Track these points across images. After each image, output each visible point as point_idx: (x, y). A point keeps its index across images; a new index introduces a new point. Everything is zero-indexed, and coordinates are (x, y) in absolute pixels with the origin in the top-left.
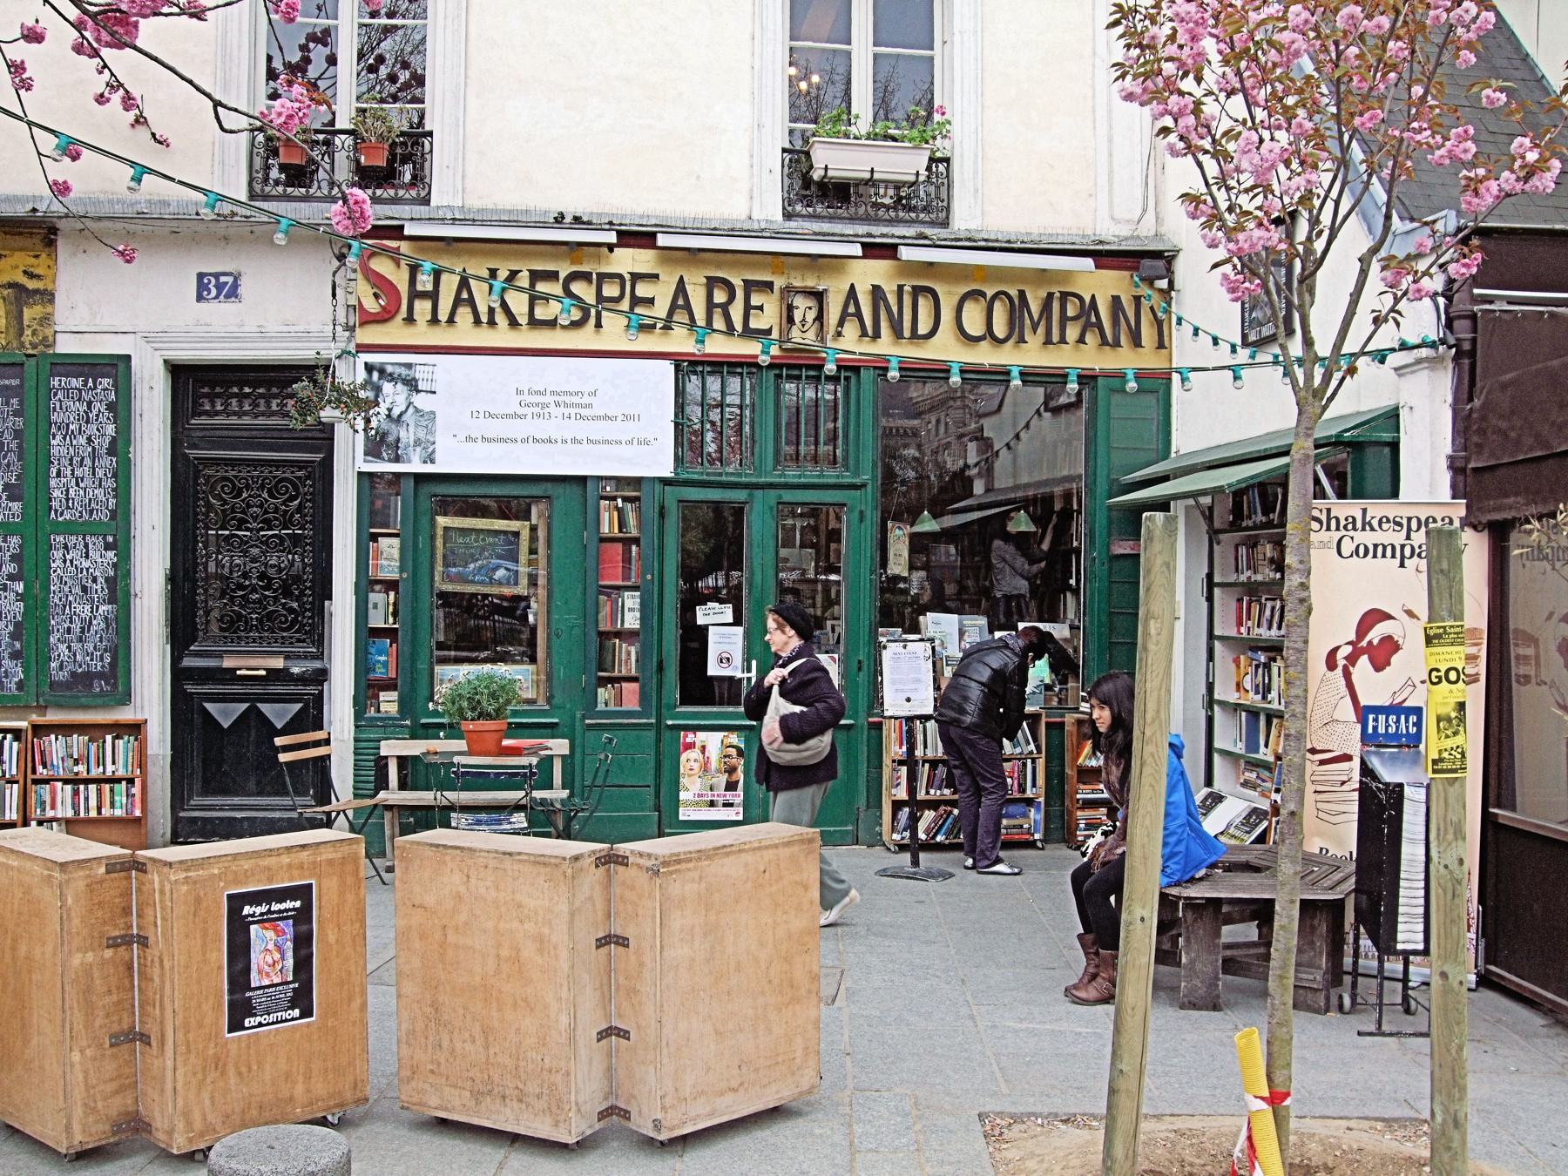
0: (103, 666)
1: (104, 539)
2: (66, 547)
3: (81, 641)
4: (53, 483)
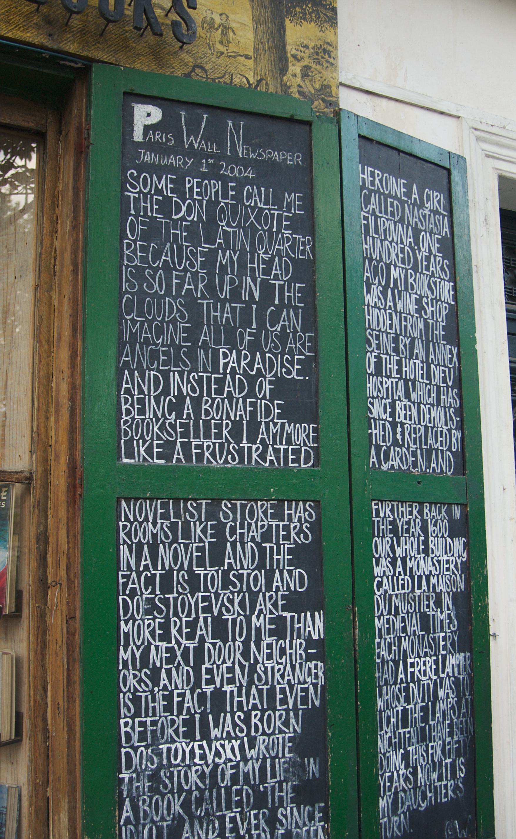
0: (456, 788)
1: (449, 512)
2: (395, 531)
3: (423, 740)
4: (371, 384)
